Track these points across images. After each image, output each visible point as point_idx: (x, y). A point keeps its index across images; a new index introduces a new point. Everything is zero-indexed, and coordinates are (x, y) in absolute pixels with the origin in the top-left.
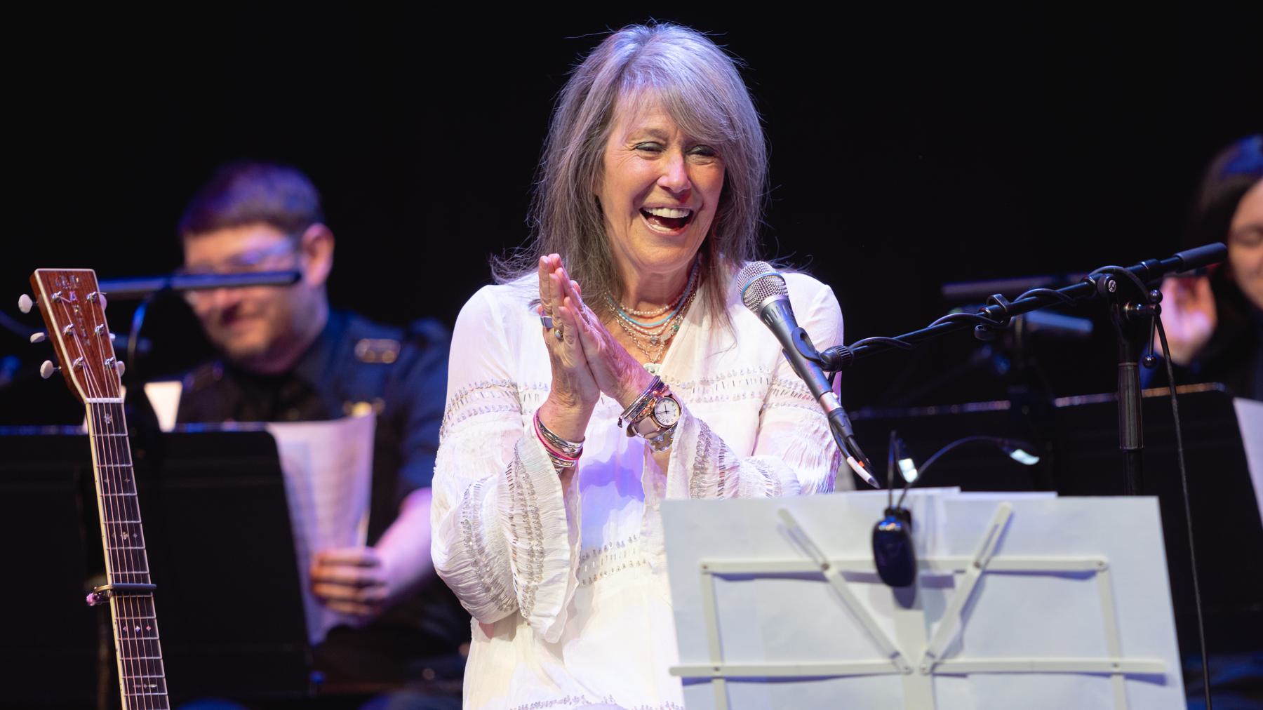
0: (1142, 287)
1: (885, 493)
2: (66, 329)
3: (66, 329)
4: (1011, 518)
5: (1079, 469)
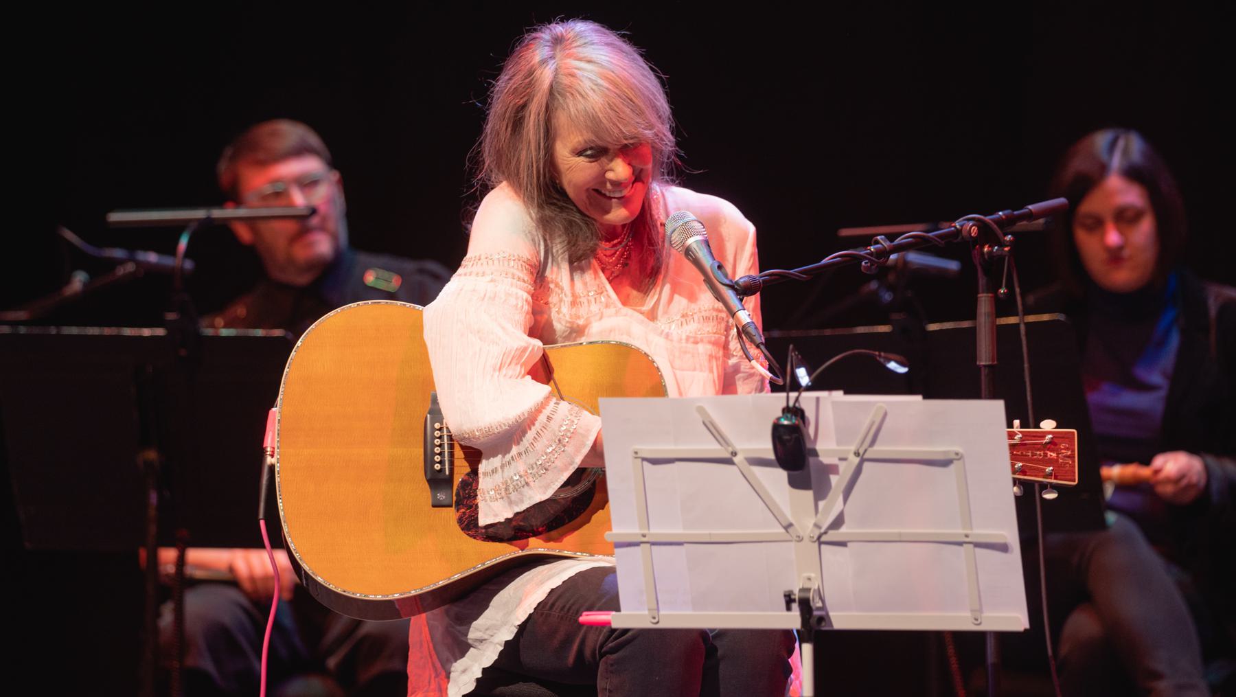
0: (999, 232)
1: (784, 395)
4: (885, 415)
5: (940, 377)
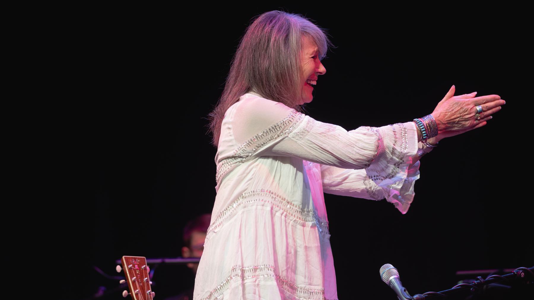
2: (133, 279)
3: (133, 279)
